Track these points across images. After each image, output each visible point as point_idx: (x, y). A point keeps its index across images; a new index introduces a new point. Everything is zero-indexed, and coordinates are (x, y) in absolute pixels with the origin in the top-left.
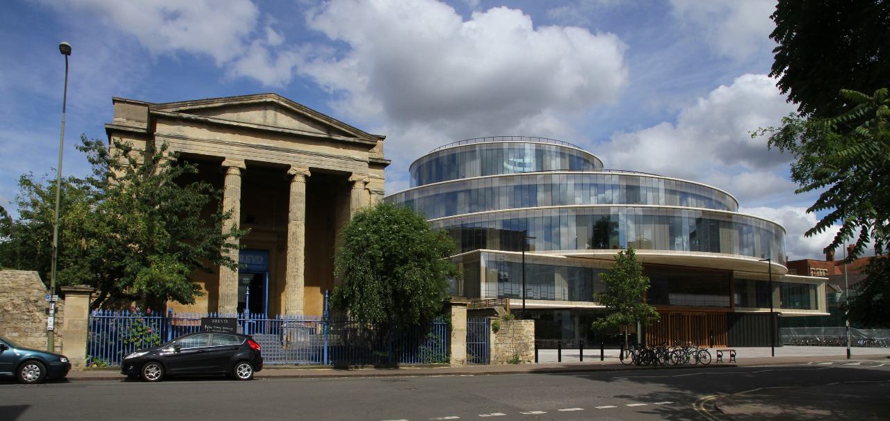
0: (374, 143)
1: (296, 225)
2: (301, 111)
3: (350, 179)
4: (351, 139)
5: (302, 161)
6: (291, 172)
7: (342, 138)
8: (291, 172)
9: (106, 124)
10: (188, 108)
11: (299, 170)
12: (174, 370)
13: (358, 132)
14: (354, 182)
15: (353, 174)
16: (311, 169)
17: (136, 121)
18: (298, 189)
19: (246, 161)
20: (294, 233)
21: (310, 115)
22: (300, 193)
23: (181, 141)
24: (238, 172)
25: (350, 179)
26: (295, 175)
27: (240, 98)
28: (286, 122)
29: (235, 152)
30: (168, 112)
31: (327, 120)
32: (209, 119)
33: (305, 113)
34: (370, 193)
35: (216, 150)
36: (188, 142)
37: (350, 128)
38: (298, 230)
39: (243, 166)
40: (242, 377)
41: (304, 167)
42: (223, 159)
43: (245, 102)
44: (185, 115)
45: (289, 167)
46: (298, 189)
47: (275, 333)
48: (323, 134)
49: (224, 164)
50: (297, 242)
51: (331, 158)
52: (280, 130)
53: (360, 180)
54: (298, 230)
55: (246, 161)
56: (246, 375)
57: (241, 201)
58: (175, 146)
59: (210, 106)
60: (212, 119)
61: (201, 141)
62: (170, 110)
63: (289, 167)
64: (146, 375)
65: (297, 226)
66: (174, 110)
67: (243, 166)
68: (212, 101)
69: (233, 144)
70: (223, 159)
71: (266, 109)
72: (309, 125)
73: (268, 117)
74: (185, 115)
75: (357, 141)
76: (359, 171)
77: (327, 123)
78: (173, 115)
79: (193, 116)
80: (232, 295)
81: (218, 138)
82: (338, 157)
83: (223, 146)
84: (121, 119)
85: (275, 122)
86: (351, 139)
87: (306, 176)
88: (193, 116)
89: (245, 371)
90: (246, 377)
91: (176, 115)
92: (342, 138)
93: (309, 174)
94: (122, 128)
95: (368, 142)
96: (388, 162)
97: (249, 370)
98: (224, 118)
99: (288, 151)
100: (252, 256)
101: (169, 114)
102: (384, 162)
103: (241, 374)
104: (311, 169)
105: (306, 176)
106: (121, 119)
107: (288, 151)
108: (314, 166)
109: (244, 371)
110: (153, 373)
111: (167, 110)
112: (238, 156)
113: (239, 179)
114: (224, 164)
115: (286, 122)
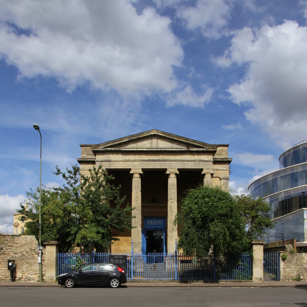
0: (215, 150)
1: (171, 202)
2: (171, 137)
3: (202, 173)
4: (201, 149)
5: (173, 165)
6: (168, 172)
7: (195, 149)
8: (168, 172)
9: (77, 159)
10: (110, 145)
11: (172, 171)
12: (79, 282)
13: (205, 144)
14: (204, 174)
15: (204, 170)
16: (179, 170)
17: (92, 155)
18: (172, 181)
19: (143, 170)
20: (170, 207)
21: (176, 139)
22: (173, 184)
23: (109, 163)
24: (138, 176)
25: (202, 173)
26: (169, 174)
27: (137, 135)
28: (163, 145)
29: (136, 165)
30: (101, 148)
31: (186, 140)
32: (121, 149)
33: (173, 138)
34: (220, 179)
35: (126, 165)
36: (112, 163)
37: (200, 143)
38: (173, 205)
39: (141, 172)
40: (113, 286)
41: (174, 169)
42: (130, 169)
44: (109, 149)
45: (166, 170)
46: (172, 181)
47: (149, 263)
48: (184, 148)
49: (131, 172)
50: (172, 212)
51: (190, 162)
52: (160, 150)
53: (208, 173)
54: (173, 205)
55: (143, 170)
56: (116, 285)
57: (141, 191)
58: (106, 166)
59: (121, 142)
60: (123, 149)
61: (118, 162)
63: (166, 170)
64: (111, 283)
65: (172, 202)
66: (104, 147)
67: (141, 172)
68: (122, 139)
69: (135, 161)
70: (130, 169)
71: (152, 139)
73: (153, 143)
74: (109, 149)
75: (205, 150)
76: (207, 167)
77: (187, 142)
78: (103, 150)
79: (113, 149)
80: (138, 243)
81: (127, 159)
82: (195, 161)
83: (130, 163)
84: (84, 155)
85: (157, 145)
86: (201, 149)
87: (176, 174)
88: (113, 149)
89: (115, 283)
90: (115, 287)
91: (104, 149)
92: (195, 149)
93: (178, 172)
94: (84, 160)
95: (211, 150)
96: (231, 160)
97: (117, 283)
98: (129, 147)
99: (165, 161)
100: (157, 221)
101: (101, 150)
102: (228, 160)
103: (113, 285)
104: (179, 170)
105: (176, 174)
106: (84, 155)
107: (165, 161)
108: (180, 167)
109: (115, 283)
110: (115, 283)
111: (100, 148)
112: (138, 167)
113: (140, 180)
114: (131, 172)
115: (163, 145)
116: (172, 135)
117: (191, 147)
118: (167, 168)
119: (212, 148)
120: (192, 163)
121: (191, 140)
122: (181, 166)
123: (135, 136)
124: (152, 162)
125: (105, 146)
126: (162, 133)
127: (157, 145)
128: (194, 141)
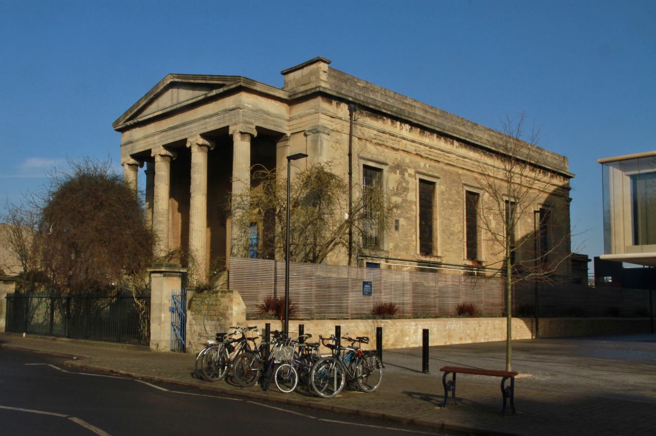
4: (221, 90)
5: (194, 128)
21: (192, 81)
43: (156, 92)
48: (200, 94)
51: (210, 117)
60: (140, 118)
62: (121, 123)
66: (124, 121)
68: (138, 103)
69: (154, 135)
72: (198, 90)
74: (128, 123)
77: (204, 82)
82: (217, 114)
86: (221, 90)
88: (131, 122)
92: (214, 92)
95: (234, 86)
99: (184, 125)
107: (184, 125)
115: (185, 96)
116: (187, 76)
117: (216, 88)
118: (187, 137)
119: (232, 82)
120: (215, 118)
121: (208, 77)
122: (202, 129)
123: (151, 94)
124: (172, 132)
125: (125, 120)
126: (177, 78)
127: (178, 100)
128: (212, 77)
